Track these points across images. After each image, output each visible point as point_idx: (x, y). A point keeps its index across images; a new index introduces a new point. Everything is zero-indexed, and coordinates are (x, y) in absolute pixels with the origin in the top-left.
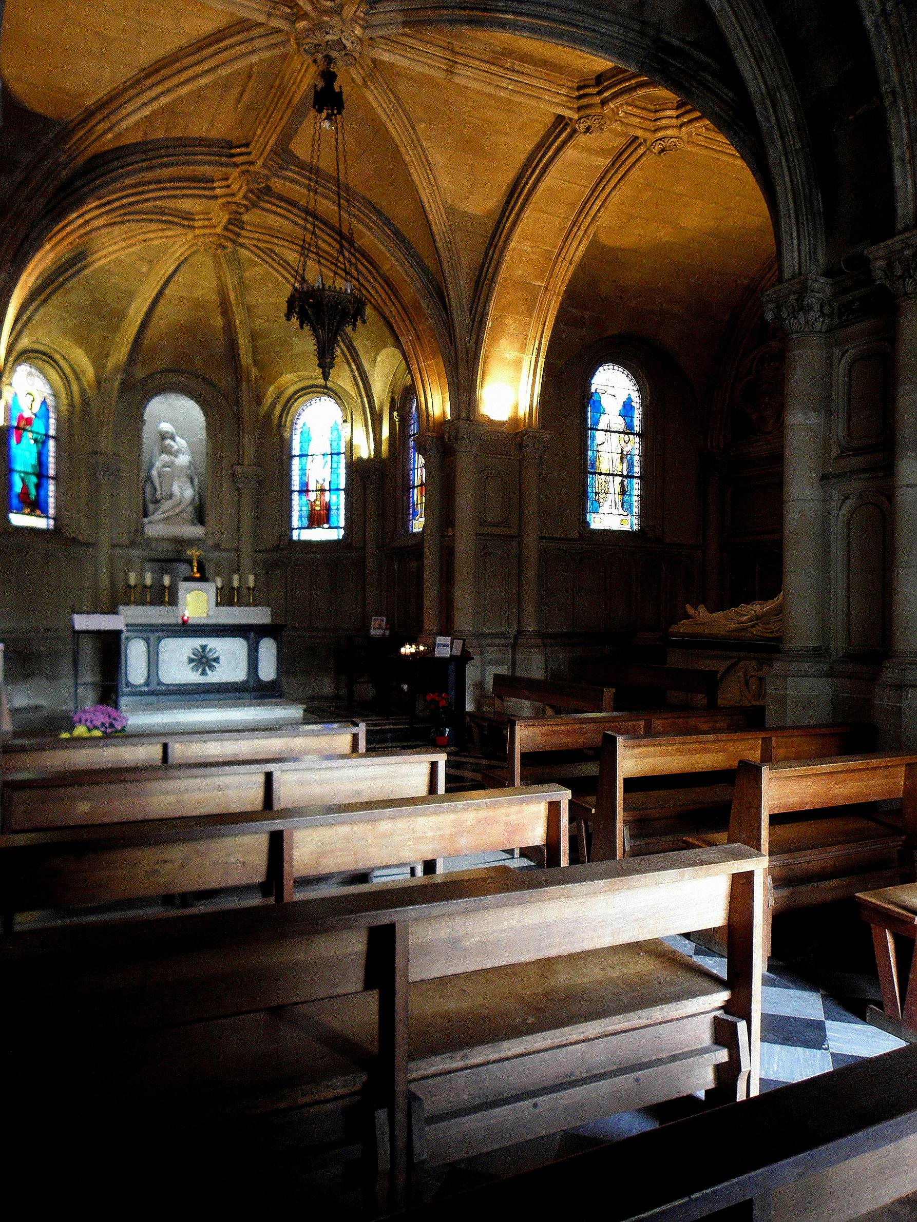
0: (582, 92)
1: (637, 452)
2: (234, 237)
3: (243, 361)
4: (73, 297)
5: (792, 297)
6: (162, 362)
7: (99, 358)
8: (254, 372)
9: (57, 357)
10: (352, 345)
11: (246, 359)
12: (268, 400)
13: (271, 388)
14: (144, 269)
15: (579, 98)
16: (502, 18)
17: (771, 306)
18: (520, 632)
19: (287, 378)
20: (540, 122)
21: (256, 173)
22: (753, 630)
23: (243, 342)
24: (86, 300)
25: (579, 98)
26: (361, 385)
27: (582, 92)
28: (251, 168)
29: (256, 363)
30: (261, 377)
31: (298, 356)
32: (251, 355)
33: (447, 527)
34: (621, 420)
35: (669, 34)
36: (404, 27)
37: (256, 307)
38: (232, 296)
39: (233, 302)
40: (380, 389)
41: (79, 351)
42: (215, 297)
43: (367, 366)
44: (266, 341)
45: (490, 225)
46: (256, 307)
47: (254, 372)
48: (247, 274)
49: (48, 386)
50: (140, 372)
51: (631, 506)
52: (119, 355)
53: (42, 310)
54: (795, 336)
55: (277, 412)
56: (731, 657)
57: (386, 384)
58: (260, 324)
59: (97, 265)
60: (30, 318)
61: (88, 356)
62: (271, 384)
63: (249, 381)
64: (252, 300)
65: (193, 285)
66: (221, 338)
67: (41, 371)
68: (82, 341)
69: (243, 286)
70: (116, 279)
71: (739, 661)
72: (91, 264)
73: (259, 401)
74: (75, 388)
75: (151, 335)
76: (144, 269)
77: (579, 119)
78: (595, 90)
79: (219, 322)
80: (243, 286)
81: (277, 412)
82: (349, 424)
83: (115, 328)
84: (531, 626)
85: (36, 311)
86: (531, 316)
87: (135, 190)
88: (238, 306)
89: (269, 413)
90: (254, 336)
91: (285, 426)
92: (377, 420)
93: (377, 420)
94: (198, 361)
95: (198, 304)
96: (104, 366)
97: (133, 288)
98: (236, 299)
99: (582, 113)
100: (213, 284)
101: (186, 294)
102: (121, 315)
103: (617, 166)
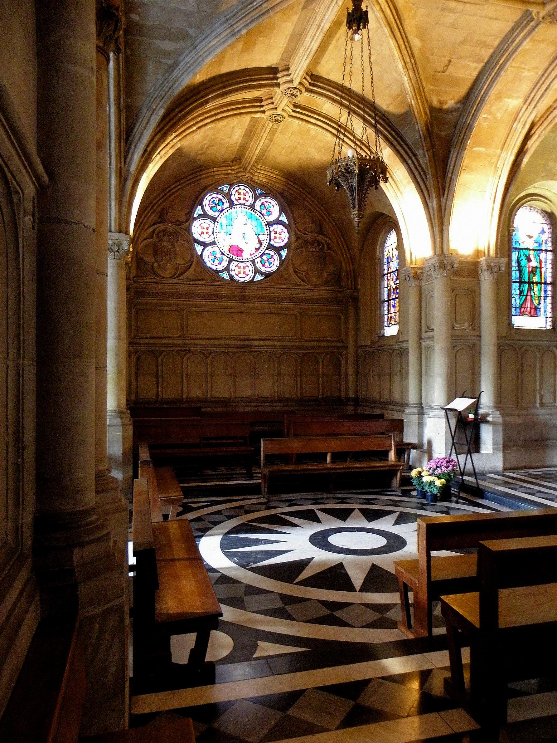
87: (544, 78)
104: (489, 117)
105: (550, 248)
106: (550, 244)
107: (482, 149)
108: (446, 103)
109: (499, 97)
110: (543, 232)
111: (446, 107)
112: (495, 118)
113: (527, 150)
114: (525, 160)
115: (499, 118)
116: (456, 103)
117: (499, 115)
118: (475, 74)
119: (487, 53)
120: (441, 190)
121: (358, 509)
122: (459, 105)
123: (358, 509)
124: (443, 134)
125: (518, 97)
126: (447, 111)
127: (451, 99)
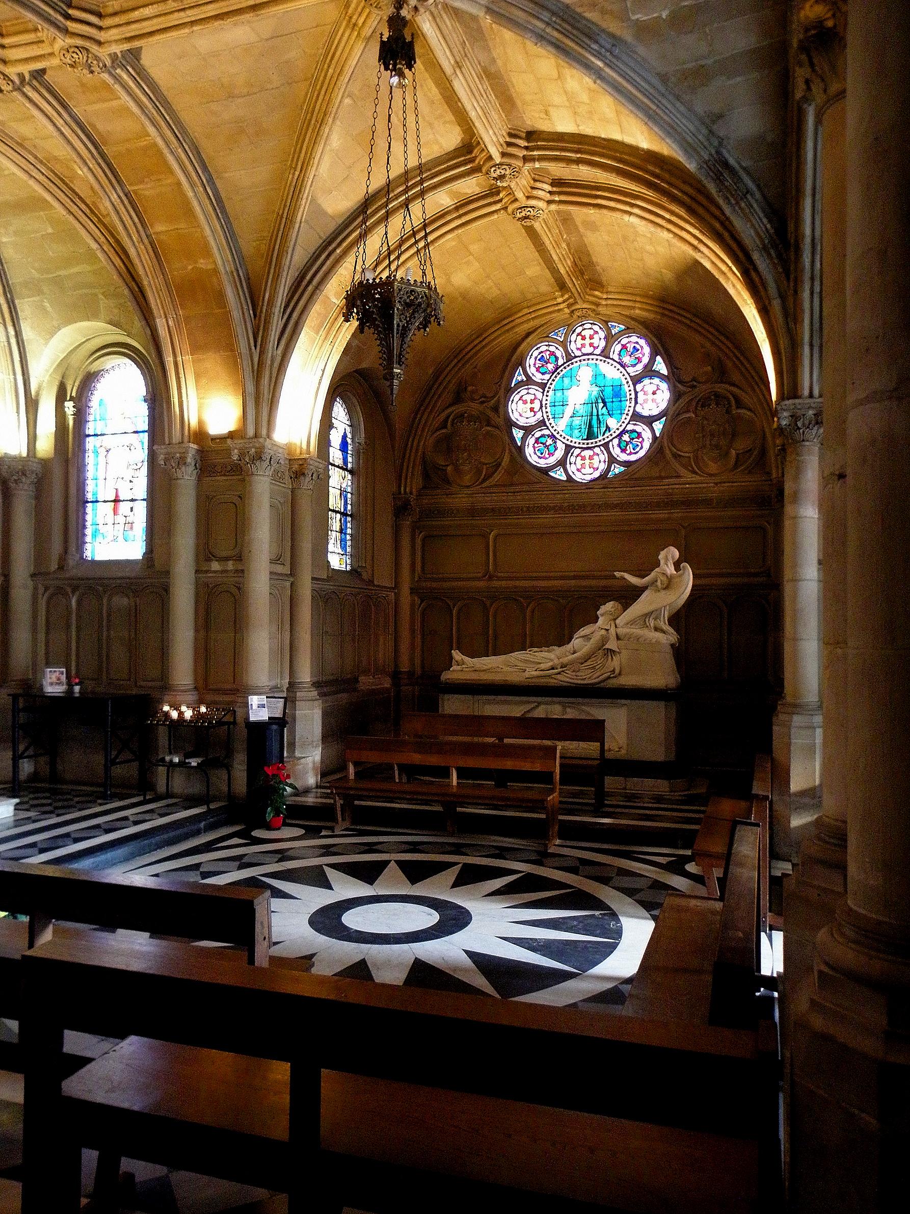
0: (513, 140)
1: (349, 490)
5: (811, 412)
15: (509, 144)
16: (588, 59)
17: (785, 414)
18: (292, 686)
20: (441, 147)
21: (97, 58)
22: (558, 676)
25: (509, 144)
27: (513, 140)
28: (94, 48)
33: (208, 560)
34: (340, 453)
35: (729, 152)
36: (486, 13)
40: (43, 370)
45: (332, 227)
51: (346, 545)
54: (807, 443)
56: (529, 702)
71: (537, 706)
77: (501, 164)
78: (523, 143)
84: (305, 675)
86: (317, 333)
99: (506, 160)
103: (461, 212)
121: (396, 861)
123: (396, 861)
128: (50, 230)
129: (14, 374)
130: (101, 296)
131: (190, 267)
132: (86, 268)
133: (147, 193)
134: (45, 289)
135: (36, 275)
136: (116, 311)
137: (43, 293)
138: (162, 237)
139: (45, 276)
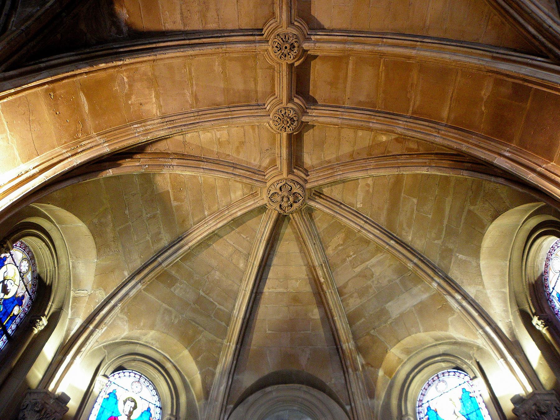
2: (301, 182)
3: (345, 346)
4: (178, 290)
6: (269, 366)
7: (207, 364)
8: (360, 360)
9: (168, 366)
10: (447, 277)
11: (348, 345)
12: (382, 394)
13: (381, 373)
14: (241, 265)
19: (395, 353)
23: (341, 325)
24: (191, 296)
26: (475, 314)
29: (359, 349)
30: (368, 364)
31: (397, 321)
32: (352, 343)
37: (345, 286)
38: (320, 273)
39: (322, 280)
40: (502, 313)
41: (186, 352)
42: (308, 289)
43: (471, 291)
44: (363, 320)
46: (345, 286)
47: (360, 360)
48: (330, 251)
49: (156, 398)
50: (248, 379)
52: (226, 359)
53: (139, 286)
55: (394, 402)
57: (505, 302)
58: (354, 303)
59: (190, 244)
60: (127, 294)
61: (195, 359)
62: (379, 367)
63: (356, 369)
64: (341, 279)
65: (287, 278)
66: (321, 332)
67: (152, 382)
68: (189, 340)
69: (329, 265)
70: (217, 275)
72: (187, 244)
73: (371, 393)
74: (183, 399)
75: (257, 338)
76: (241, 265)
79: (316, 314)
80: (329, 265)
81: (394, 402)
82: (480, 378)
83: (223, 333)
85: (133, 287)
88: (328, 287)
89: (387, 405)
90: (352, 319)
91: (407, 414)
92: (514, 347)
93: (514, 347)
94: (303, 361)
95: (295, 299)
96: (213, 374)
97: (235, 287)
98: (325, 278)
100: (303, 273)
101: (281, 290)
102: (228, 318)
104: (127, 86)
105: (10, 332)
106: (14, 326)
107: (87, 108)
108: (122, 6)
109: (153, 82)
110: (18, 300)
111: (117, 8)
112: (128, 96)
113: (120, 165)
114: (110, 172)
115: (130, 102)
116: (127, 24)
117: (133, 97)
118: (169, 26)
119: (195, 25)
120: (11, 60)
122: (125, 29)
124: (83, 27)
125: (160, 107)
126: (113, 15)
127: (128, 11)
128: (415, 201)
129: (482, 328)
130: (472, 208)
131: (483, 108)
132: (449, 200)
133: (418, 103)
134: (451, 246)
135: (438, 242)
136: (487, 205)
137: (451, 251)
138: (452, 116)
139: (443, 236)
